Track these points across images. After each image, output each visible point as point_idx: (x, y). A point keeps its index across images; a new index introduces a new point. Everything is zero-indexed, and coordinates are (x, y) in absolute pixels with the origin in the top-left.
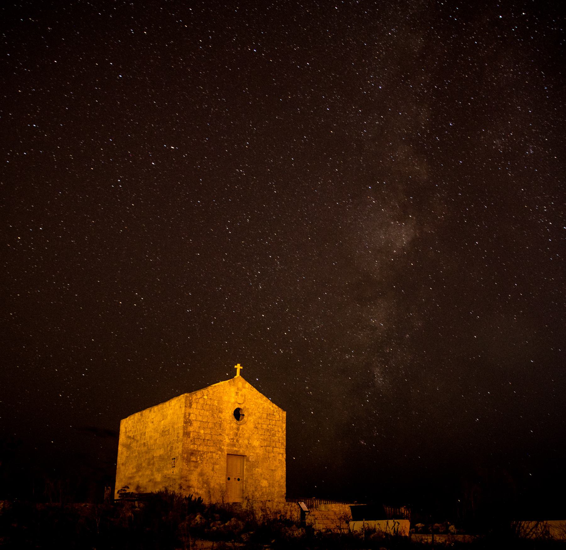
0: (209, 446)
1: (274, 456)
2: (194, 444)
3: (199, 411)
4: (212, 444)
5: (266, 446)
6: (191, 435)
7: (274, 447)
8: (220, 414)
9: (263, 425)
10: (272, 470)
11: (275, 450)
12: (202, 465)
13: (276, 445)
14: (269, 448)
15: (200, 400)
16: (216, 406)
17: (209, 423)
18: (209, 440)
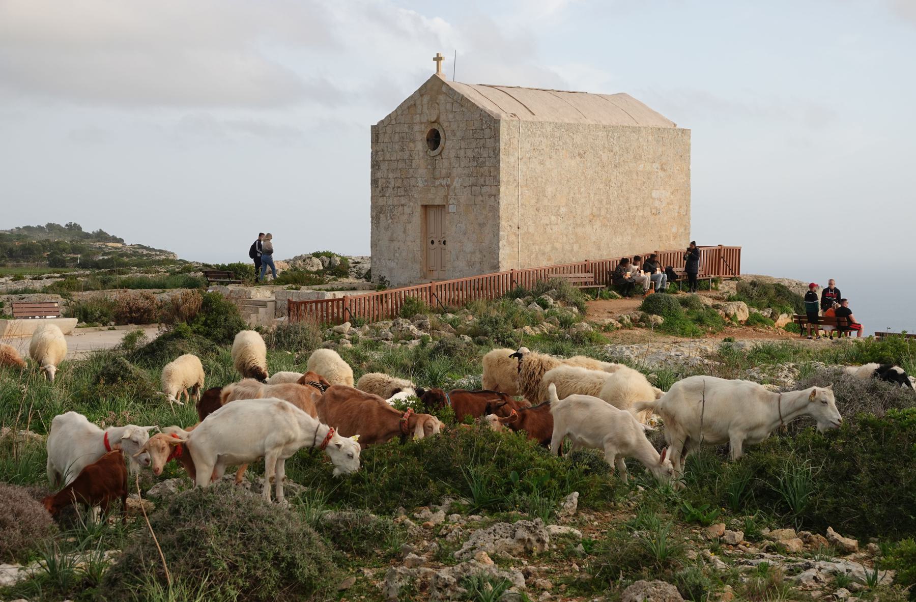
0: (400, 196)
1: (483, 201)
2: (383, 196)
3: (386, 145)
4: (403, 193)
5: (471, 186)
6: (380, 184)
7: (483, 186)
8: (411, 145)
9: (467, 151)
10: (480, 225)
11: (485, 189)
12: (392, 226)
13: (485, 181)
14: (476, 188)
15: (387, 128)
16: (406, 133)
17: (398, 161)
18: (399, 187)
